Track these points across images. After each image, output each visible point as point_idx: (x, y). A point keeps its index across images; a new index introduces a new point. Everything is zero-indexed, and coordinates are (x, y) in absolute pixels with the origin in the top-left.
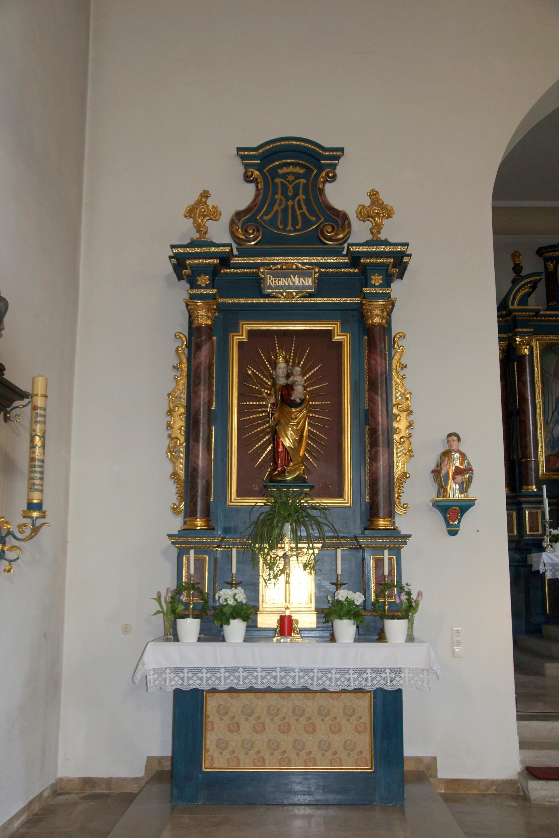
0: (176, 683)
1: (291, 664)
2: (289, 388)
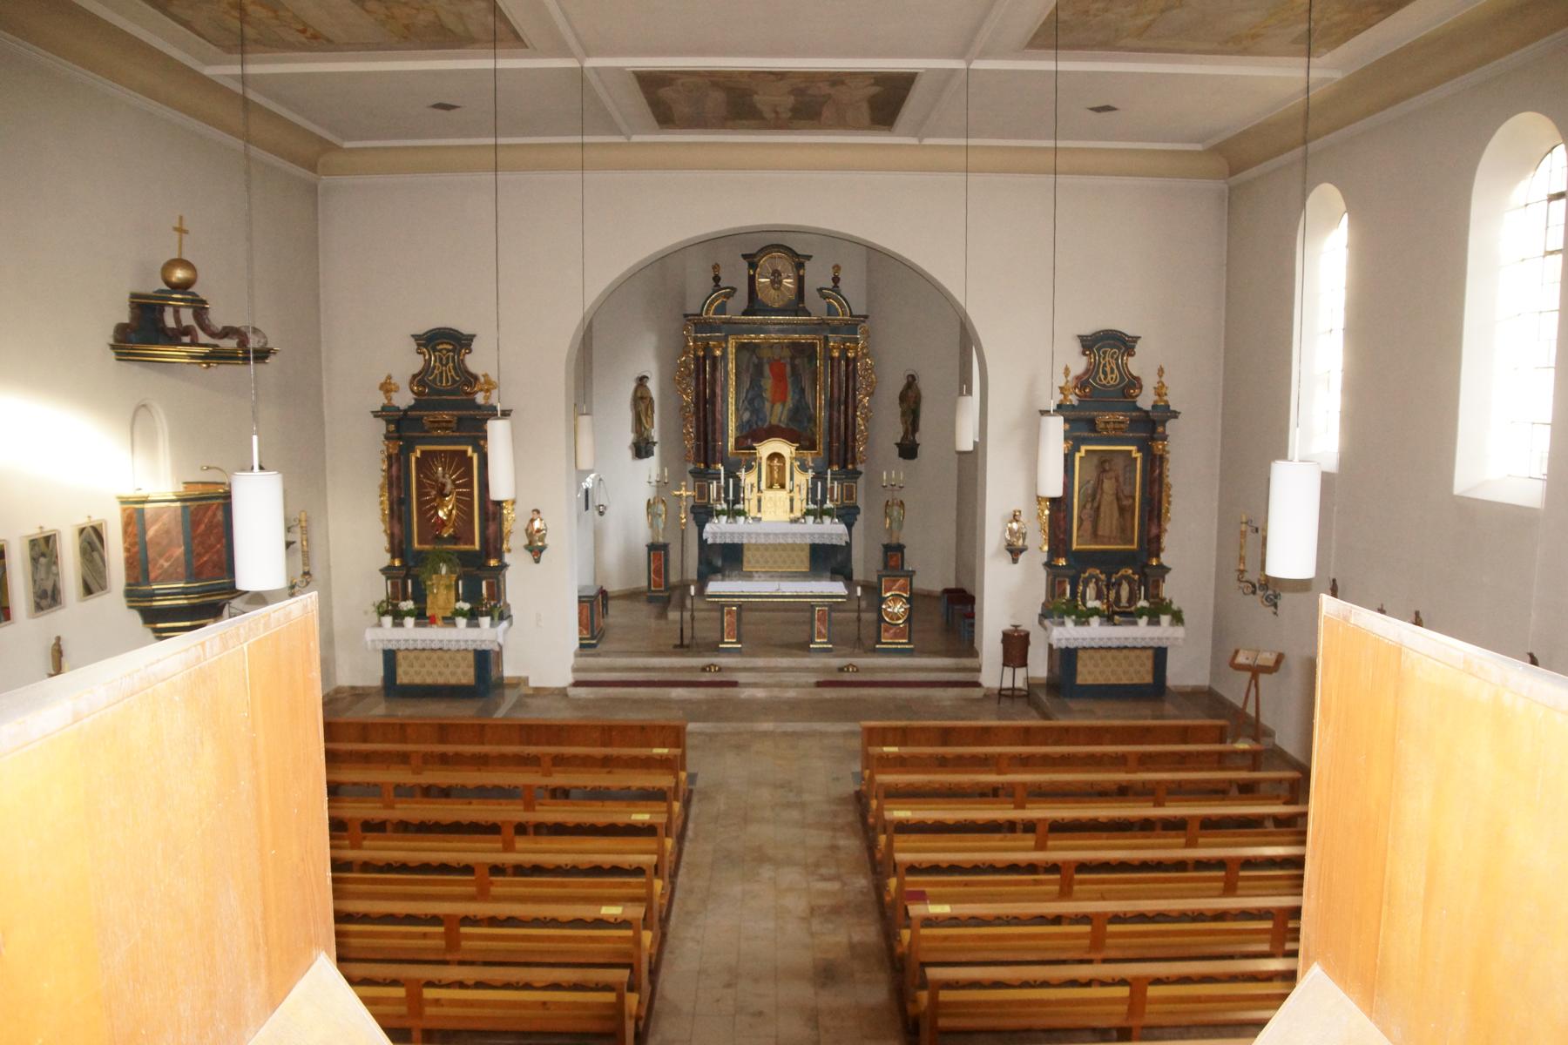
0: (380, 646)
1: (434, 637)
2: (444, 485)
